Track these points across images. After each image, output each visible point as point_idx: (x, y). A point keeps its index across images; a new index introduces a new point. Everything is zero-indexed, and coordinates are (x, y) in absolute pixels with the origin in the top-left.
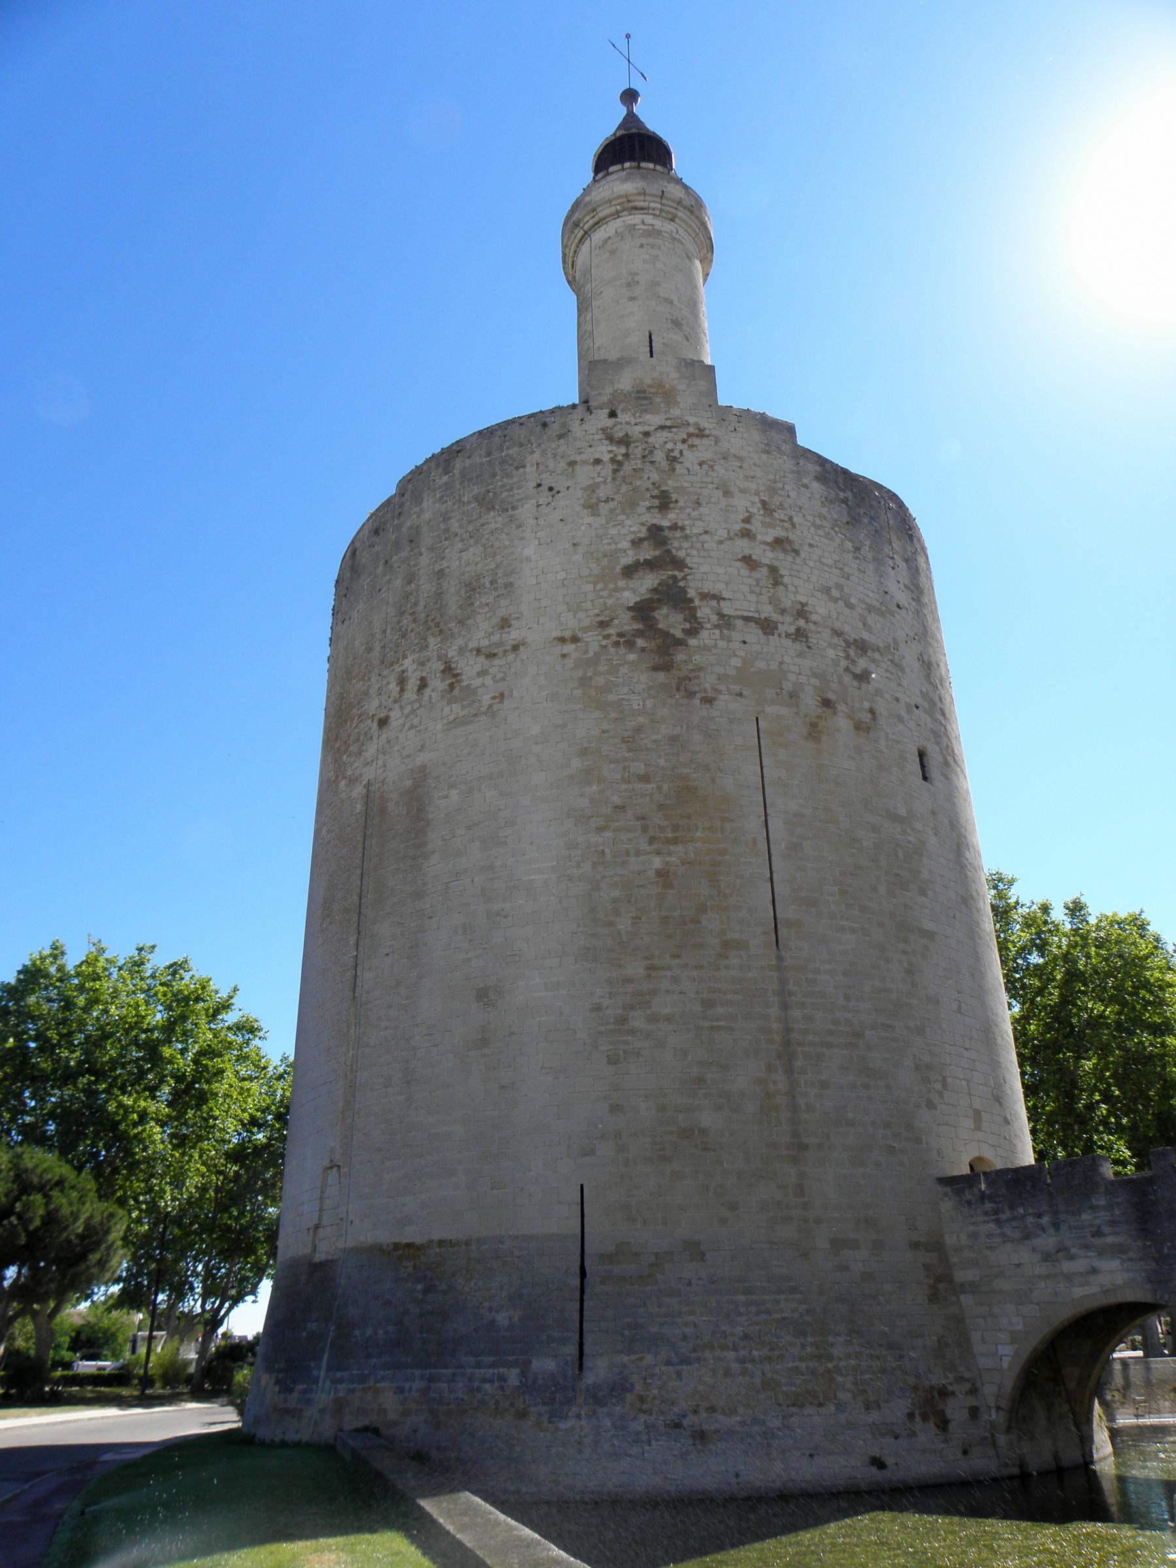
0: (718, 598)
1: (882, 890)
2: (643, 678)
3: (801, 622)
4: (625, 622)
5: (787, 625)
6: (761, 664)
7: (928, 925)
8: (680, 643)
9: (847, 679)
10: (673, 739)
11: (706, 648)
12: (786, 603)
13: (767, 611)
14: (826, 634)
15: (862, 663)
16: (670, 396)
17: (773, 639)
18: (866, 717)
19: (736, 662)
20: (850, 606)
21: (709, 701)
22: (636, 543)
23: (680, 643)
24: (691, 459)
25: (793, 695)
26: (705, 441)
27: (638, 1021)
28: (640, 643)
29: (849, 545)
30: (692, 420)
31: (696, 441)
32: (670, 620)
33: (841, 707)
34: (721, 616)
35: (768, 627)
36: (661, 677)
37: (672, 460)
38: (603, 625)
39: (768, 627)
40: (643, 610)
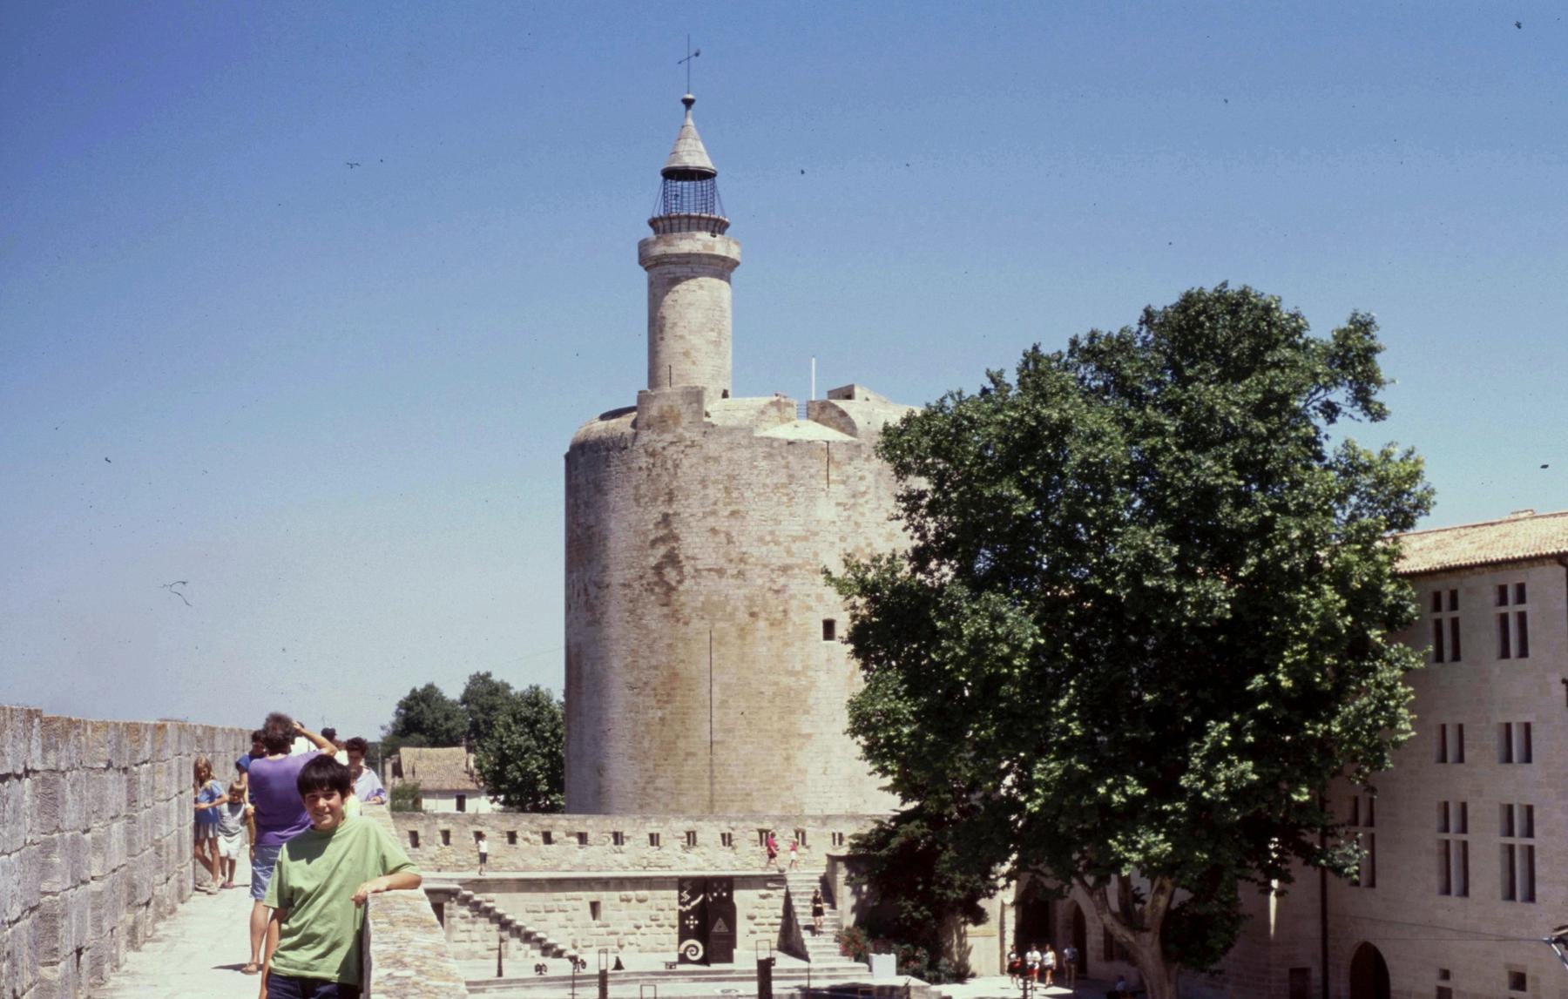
0: (694, 558)
1: (775, 718)
2: (658, 611)
3: (742, 566)
4: (651, 576)
5: (732, 570)
6: (715, 598)
7: (806, 729)
8: (674, 589)
9: (769, 595)
10: (670, 645)
11: (687, 591)
12: (734, 555)
13: (722, 562)
14: (758, 570)
15: (782, 581)
16: (677, 420)
17: (724, 581)
18: (779, 616)
19: (701, 598)
20: (777, 543)
21: (686, 624)
22: (657, 525)
23: (674, 589)
24: (686, 463)
25: (732, 615)
26: (694, 450)
27: (650, 790)
28: (657, 589)
29: (785, 499)
30: (687, 435)
31: (688, 451)
32: (671, 575)
33: (763, 615)
34: (697, 570)
35: (721, 572)
36: (666, 610)
37: (676, 466)
38: (641, 577)
39: (721, 572)
40: (658, 569)
